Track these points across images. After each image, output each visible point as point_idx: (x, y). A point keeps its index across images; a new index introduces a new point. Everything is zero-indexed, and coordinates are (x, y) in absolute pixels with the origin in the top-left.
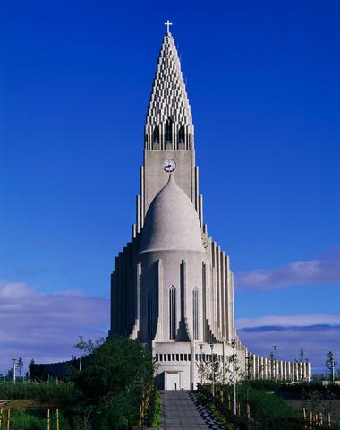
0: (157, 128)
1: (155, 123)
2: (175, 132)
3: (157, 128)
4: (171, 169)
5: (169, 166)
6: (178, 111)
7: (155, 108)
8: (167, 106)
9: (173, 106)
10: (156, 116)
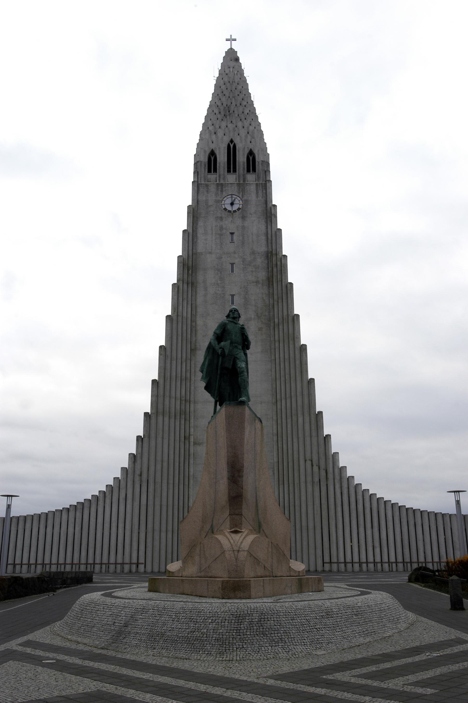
0: (212, 153)
2: (241, 158)
3: (212, 153)
4: (235, 207)
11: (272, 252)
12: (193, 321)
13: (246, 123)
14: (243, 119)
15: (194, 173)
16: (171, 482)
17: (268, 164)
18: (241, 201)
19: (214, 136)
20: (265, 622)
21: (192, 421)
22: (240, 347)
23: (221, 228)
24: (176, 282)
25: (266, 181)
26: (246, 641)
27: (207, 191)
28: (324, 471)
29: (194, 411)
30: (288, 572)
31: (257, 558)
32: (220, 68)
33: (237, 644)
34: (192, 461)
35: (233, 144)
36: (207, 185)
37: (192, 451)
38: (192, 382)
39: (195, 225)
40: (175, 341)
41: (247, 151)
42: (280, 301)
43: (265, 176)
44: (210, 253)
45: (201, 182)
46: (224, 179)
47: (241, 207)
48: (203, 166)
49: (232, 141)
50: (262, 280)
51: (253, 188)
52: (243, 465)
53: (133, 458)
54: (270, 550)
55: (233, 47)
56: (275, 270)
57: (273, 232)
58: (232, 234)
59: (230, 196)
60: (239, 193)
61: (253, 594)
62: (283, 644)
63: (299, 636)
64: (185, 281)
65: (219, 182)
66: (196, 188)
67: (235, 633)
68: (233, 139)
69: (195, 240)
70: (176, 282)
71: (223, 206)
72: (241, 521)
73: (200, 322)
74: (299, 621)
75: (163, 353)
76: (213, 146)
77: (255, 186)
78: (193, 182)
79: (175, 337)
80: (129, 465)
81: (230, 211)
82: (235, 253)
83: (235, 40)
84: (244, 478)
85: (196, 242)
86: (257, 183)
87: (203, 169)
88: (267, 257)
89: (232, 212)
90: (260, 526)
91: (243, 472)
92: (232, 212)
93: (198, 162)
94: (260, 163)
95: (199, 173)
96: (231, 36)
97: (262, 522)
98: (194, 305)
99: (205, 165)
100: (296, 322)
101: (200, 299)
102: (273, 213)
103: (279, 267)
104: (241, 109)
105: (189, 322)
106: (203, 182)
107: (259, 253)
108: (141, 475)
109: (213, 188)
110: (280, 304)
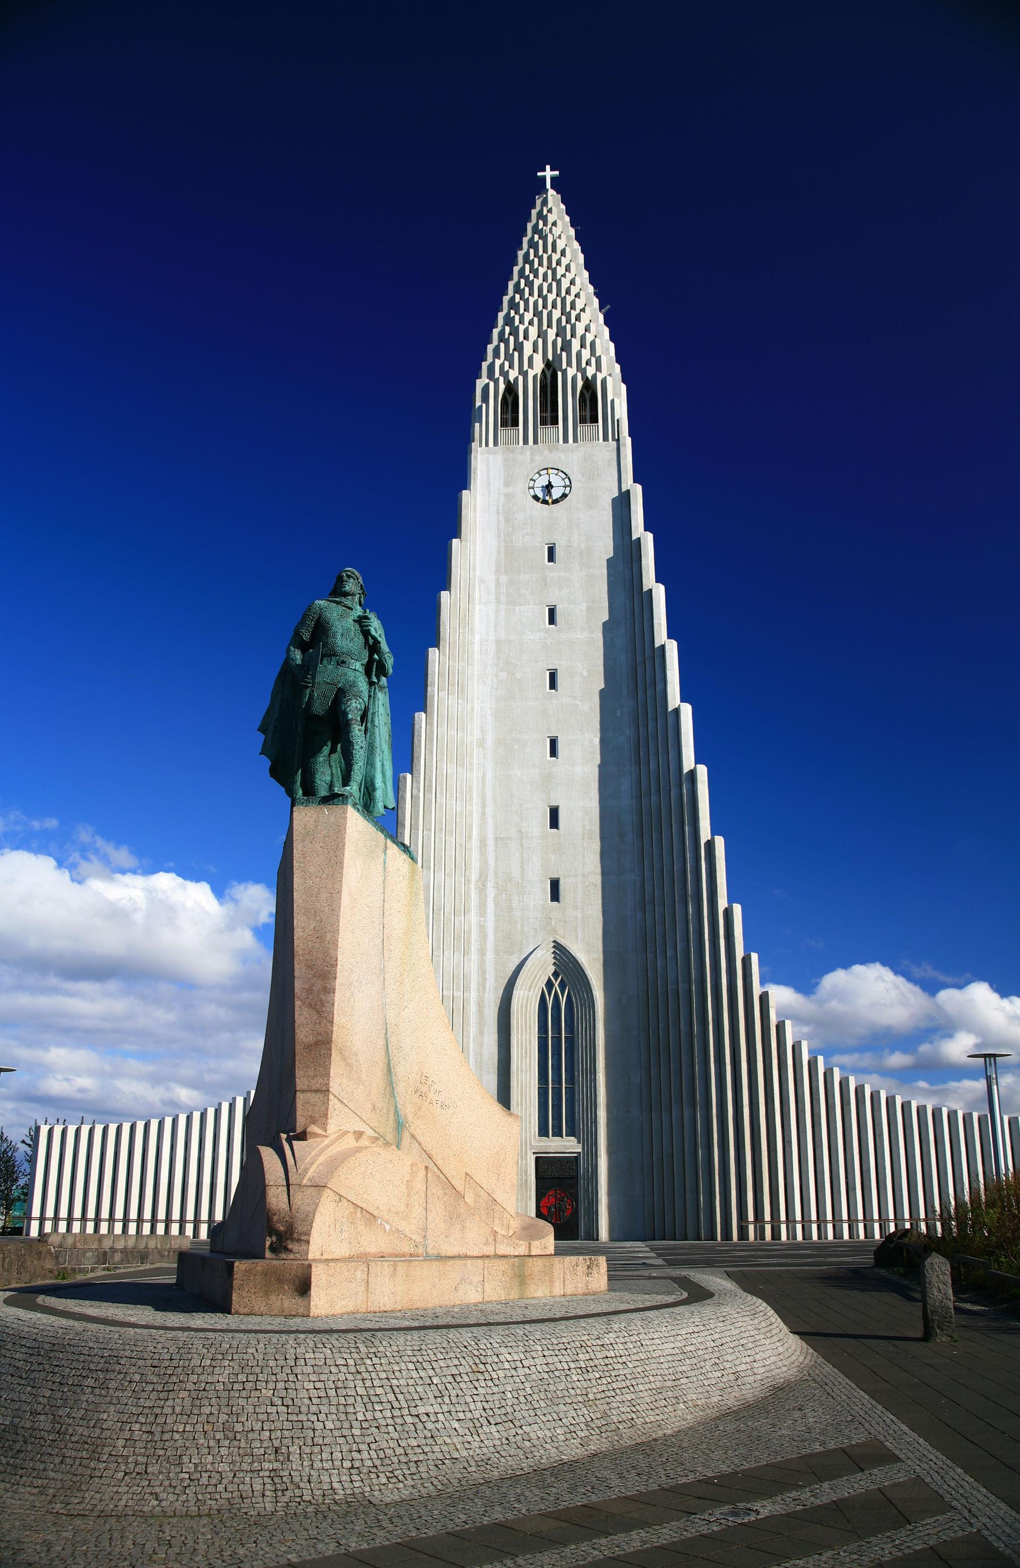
0: (511, 389)
1: (505, 374)
3: (511, 389)
4: (556, 493)
5: (549, 487)
6: (576, 344)
7: (507, 343)
8: (542, 334)
9: (561, 332)
10: (509, 358)
18: (568, 483)
20: (244, 1394)
22: (358, 666)
26: (161, 1452)
30: (486, 1243)
31: (364, 1206)
33: (130, 1460)
35: (551, 370)
41: (580, 383)
47: (567, 492)
49: (548, 365)
52: (337, 960)
54: (419, 1185)
61: (235, 1306)
62: (277, 1465)
63: (342, 1440)
67: (142, 1424)
72: (327, 1109)
74: (361, 1391)
84: (337, 994)
89: (550, 501)
90: (400, 1126)
91: (335, 978)
92: (550, 501)
97: (410, 1118)
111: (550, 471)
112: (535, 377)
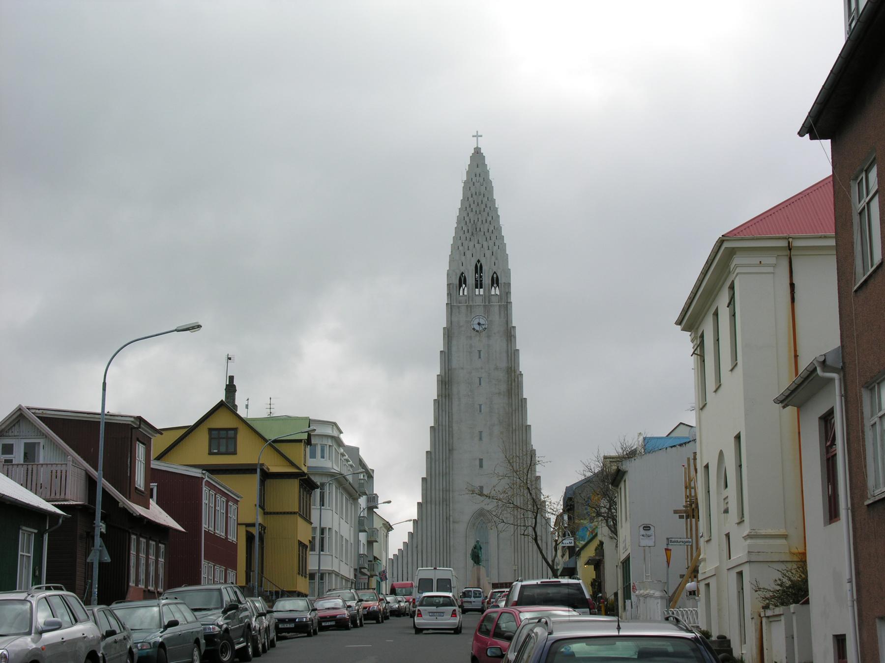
2: (487, 281)
11: (511, 367)
12: (450, 426)
13: (491, 243)
14: (488, 238)
15: (448, 294)
16: (438, 550)
17: (509, 284)
19: (464, 257)
21: (451, 505)
23: (471, 346)
24: (436, 398)
25: (507, 302)
27: (459, 312)
28: (546, 544)
29: (453, 497)
32: (467, 169)
34: (451, 535)
36: (459, 307)
37: (451, 528)
38: (451, 475)
39: (450, 343)
40: (437, 446)
42: (517, 411)
43: (506, 298)
44: (462, 369)
45: (453, 303)
46: (472, 301)
48: (455, 287)
49: (479, 261)
50: (504, 392)
51: (496, 309)
53: (411, 535)
55: (479, 147)
56: (513, 384)
57: (512, 352)
58: (480, 352)
59: (478, 317)
60: (485, 314)
64: (444, 396)
65: (469, 303)
66: (450, 310)
68: (480, 260)
69: (450, 358)
70: (436, 398)
71: (472, 326)
73: (455, 427)
75: (429, 456)
76: (462, 269)
77: (498, 307)
78: (447, 304)
79: (437, 443)
80: (408, 540)
81: (477, 331)
82: (482, 368)
83: (481, 136)
85: (451, 359)
86: (500, 306)
87: (455, 291)
88: (508, 371)
93: (450, 284)
94: (503, 285)
95: (452, 296)
96: (477, 132)
98: (450, 414)
99: (457, 287)
100: (528, 431)
101: (455, 408)
102: (512, 334)
103: (516, 382)
104: (486, 225)
105: (447, 429)
106: (455, 304)
107: (501, 369)
108: (417, 547)
109: (463, 310)
110: (517, 414)
111: (481, 317)
112: (473, 270)
